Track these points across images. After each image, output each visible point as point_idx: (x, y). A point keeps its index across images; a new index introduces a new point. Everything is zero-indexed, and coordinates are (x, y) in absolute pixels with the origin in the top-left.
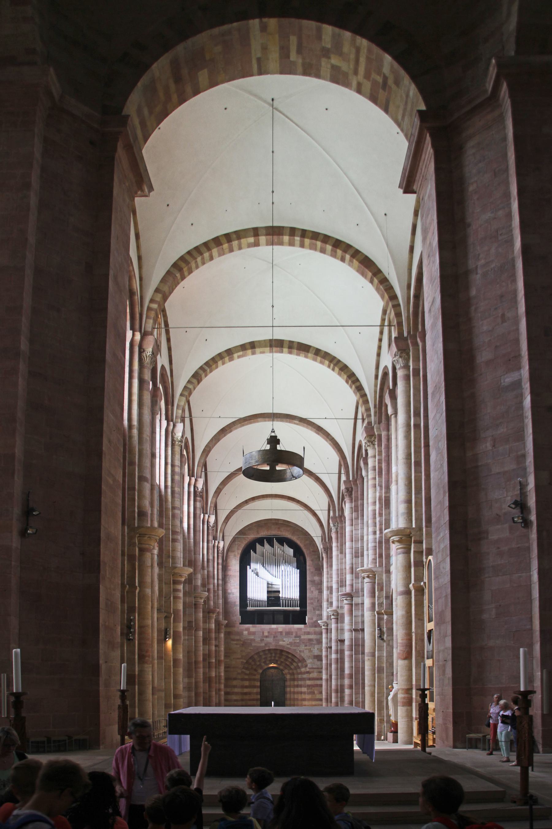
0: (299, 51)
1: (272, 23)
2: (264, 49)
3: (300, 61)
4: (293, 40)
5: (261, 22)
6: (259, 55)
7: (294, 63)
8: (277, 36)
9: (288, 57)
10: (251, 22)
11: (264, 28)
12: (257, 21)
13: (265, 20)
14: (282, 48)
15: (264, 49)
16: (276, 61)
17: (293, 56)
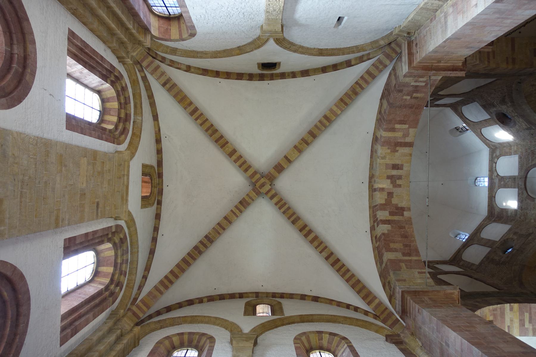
0: (530, 322)
1: (516, 306)
2: (512, 320)
3: (531, 327)
4: (527, 315)
5: (510, 306)
6: (509, 324)
7: (527, 329)
8: (518, 314)
9: (524, 325)
10: (506, 305)
11: (511, 309)
12: (508, 304)
13: (512, 304)
14: (520, 320)
15: (512, 320)
16: (517, 328)
17: (527, 325)
